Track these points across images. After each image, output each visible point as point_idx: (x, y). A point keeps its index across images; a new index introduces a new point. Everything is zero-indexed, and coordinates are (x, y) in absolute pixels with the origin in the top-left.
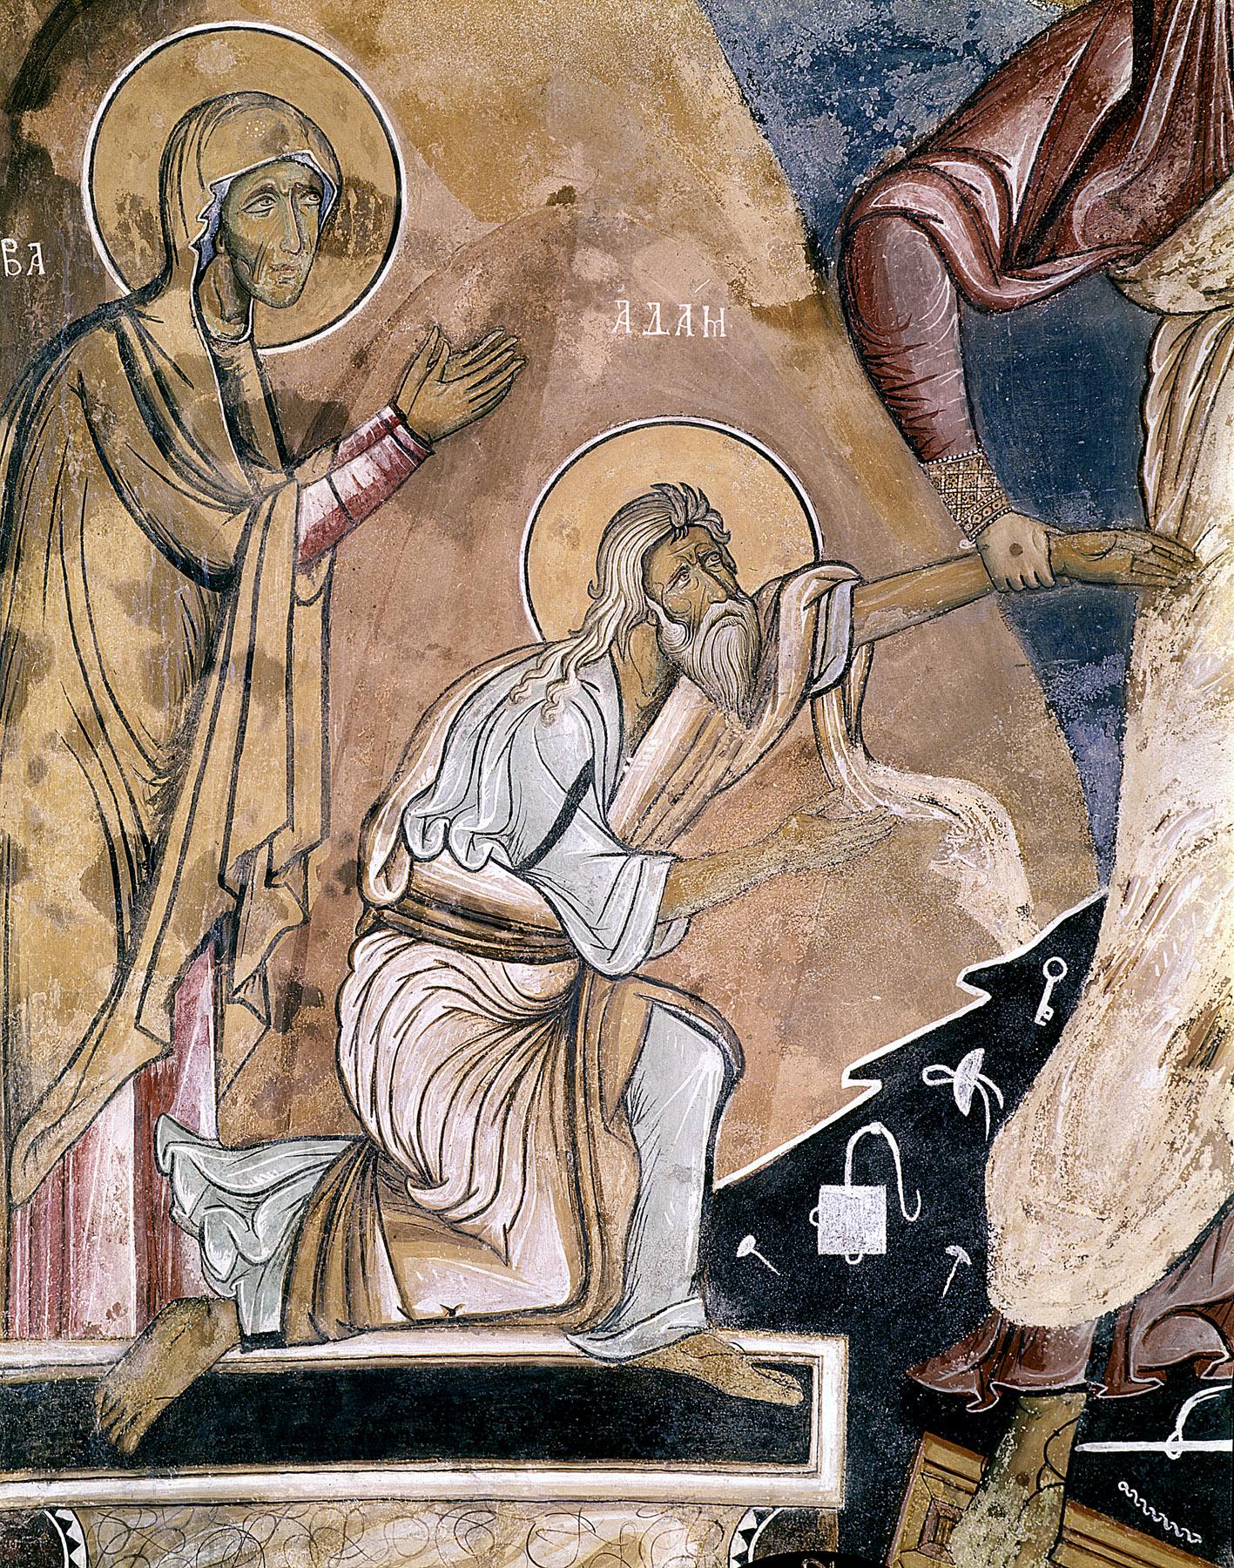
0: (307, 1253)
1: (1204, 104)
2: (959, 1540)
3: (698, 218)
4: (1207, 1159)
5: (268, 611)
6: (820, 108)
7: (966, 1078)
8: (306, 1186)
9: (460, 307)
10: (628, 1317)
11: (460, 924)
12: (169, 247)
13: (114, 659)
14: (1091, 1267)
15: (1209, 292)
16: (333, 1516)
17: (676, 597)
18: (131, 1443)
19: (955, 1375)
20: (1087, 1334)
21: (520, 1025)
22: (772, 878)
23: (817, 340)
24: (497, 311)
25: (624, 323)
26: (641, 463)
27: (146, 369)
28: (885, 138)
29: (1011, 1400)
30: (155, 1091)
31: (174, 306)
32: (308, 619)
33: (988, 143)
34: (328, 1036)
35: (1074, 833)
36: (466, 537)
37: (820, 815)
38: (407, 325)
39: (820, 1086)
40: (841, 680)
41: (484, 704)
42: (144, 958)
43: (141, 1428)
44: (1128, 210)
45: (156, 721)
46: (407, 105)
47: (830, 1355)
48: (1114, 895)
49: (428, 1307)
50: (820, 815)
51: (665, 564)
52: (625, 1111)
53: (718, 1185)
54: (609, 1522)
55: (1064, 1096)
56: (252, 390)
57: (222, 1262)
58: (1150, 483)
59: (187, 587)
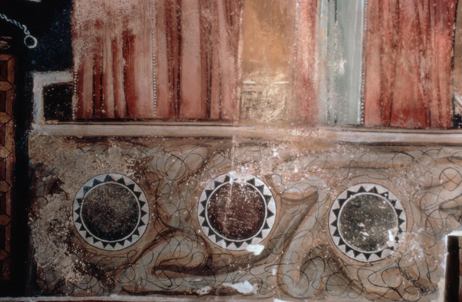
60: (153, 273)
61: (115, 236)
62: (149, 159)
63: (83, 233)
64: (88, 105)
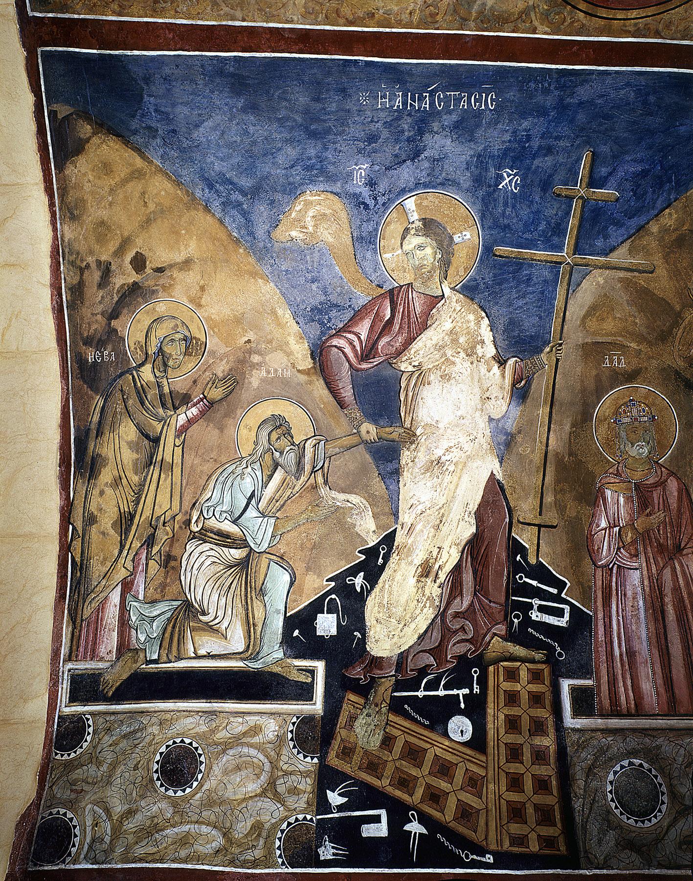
0: (167, 635)
1: (409, 320)
2: (357, 724)
3: (283, 347)
4: (428, 605)
5: (168, 449)
6: (313, 320)
7: (359, 581)
8: (168, 615)
9: (221, 369)
10: (261, 655)
11: (217, 537)
12: (147, 353)
13: (125, 462)
14: (396, 639)
15: (414, 366)
16: (168, 716)
17: (277, 445)
18: (110, 693)
19: (357, 672)
20: (395, 658)
21: (231, 567)
22: (304, 524)
23: (314, 378)
24: (231, 370)
25: (264, 373)
26: (267, 409)
27: (139, 385)
28: (330, 328)
29: (373, 678)
30: (127, 586)
31: (148, 368)
32: (178, 451)
33: (356, 329)
34: (177, 570)
35: (387, 510)
36: (221, 429)
37: (317, 505)
38: (207, 374)
39: (316, 585)
40: (322, 467)
41: (225, 474)
42: (127, 547)
43: (114, 689)
44: (392, 346)
45: (135, 479)
46: (209, 319)
47: (320, 666)
48: (399, 527)
49: (202, 652)
50: (317, 505)
51: (274, 436)
52: (262, 592)
53: (288, 615)
54: (252, 720)
55: (387, 586)
56: (166, 390)
57: (142, 638)
58: (403, 414)
59: (146, 442)
60: (680, 848)
61: (643, 814)
62: (659, 747)
63: (617, 812)
64: (606, 703)
